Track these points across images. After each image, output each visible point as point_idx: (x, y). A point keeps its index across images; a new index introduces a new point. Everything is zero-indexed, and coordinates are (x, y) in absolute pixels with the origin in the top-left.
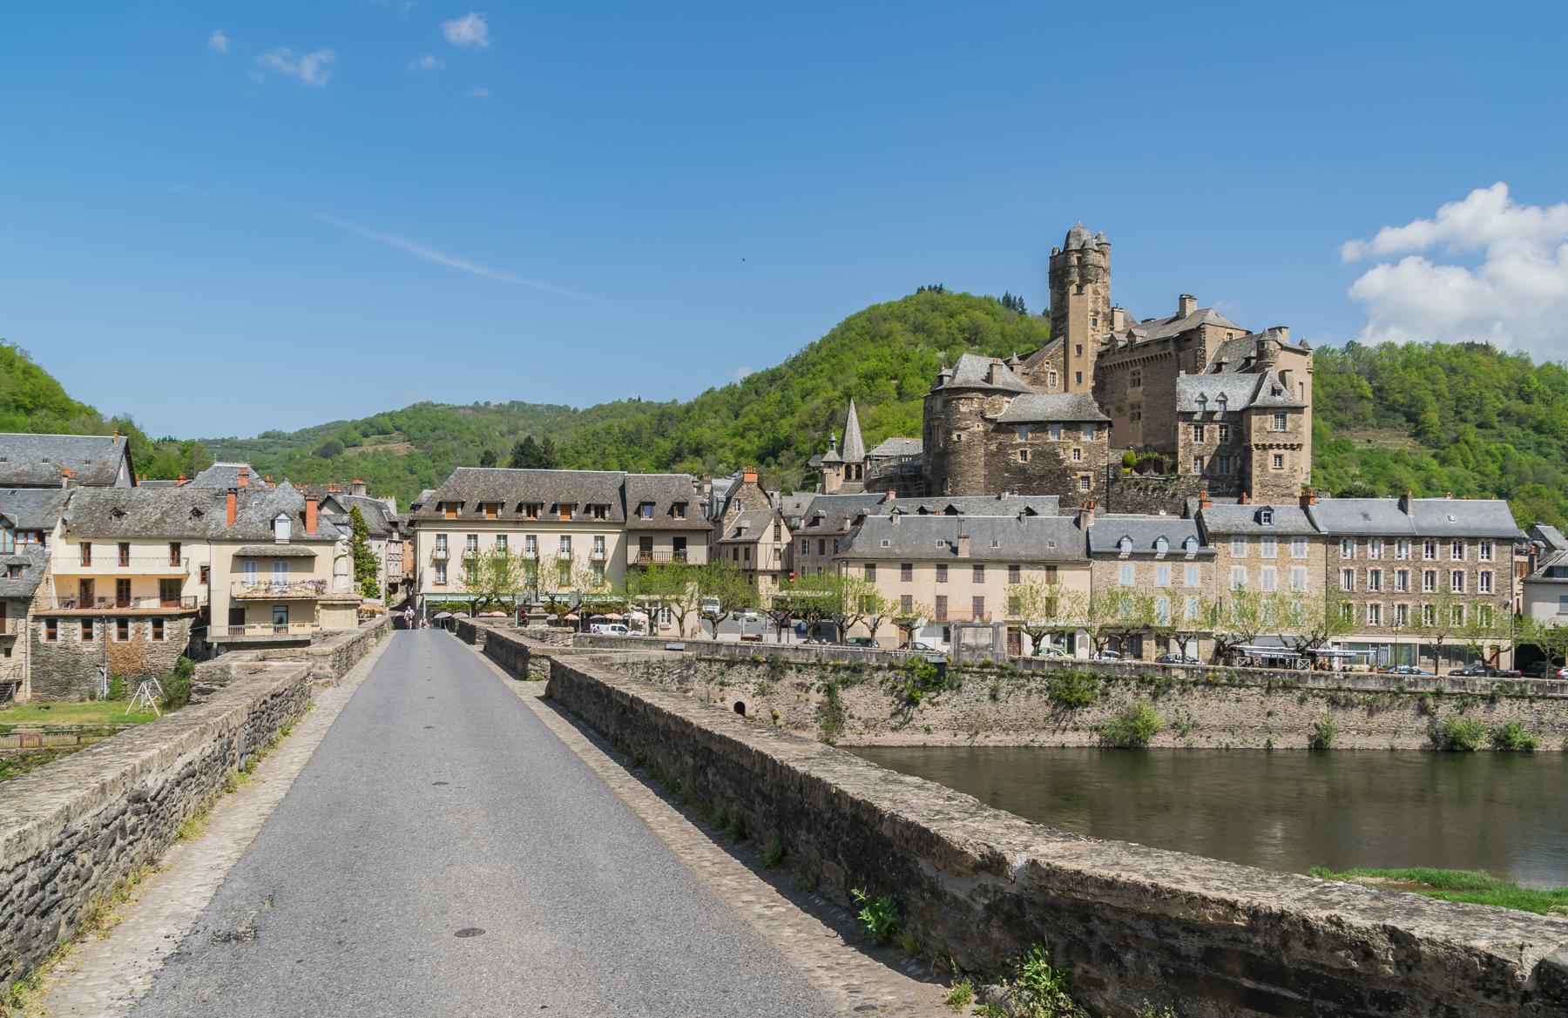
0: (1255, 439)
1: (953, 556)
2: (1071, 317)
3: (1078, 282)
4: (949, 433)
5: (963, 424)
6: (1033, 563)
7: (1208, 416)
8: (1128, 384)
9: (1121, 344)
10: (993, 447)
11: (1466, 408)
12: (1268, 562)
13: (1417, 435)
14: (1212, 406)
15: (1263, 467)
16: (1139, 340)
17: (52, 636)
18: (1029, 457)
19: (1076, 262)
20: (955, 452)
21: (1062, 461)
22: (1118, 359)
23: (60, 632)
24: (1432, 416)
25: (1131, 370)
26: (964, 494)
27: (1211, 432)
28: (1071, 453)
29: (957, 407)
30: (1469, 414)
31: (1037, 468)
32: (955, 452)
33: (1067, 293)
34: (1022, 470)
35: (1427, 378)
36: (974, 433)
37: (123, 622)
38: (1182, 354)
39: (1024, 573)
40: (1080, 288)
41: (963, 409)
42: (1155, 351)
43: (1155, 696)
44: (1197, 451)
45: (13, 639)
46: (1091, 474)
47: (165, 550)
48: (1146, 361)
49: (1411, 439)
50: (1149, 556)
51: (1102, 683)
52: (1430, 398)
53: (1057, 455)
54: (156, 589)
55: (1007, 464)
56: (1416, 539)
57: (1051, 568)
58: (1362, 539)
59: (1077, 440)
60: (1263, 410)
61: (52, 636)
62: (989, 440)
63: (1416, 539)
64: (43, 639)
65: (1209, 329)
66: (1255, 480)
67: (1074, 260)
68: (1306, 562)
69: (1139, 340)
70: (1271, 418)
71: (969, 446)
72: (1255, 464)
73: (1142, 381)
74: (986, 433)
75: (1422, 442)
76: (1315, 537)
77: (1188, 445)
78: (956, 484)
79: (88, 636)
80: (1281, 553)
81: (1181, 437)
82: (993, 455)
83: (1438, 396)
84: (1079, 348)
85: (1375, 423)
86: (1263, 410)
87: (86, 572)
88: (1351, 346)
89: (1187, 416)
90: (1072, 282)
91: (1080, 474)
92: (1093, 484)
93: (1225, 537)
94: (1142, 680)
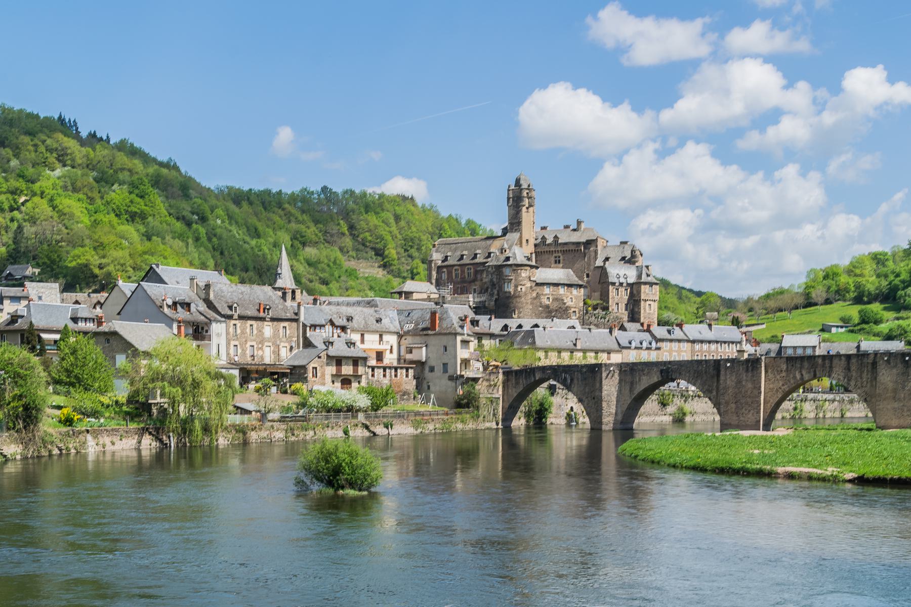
0: (642, 298)
1: (574, 347)
2: (524, 224)
3: (527, 206)
4: (516, 286)
5: (523, 283)
6: (603, 351)
7: (621, 284)
8: (553, 262)
9: (548, 242)
10: (534, 295)
11: (412, 247)
12: (675, 351)
13: (384, 266)
14: (622, 280)
15: (645, 309)
16: (560, 241)
17: (373, 375)
18: (551, 300)
19: (526, 195)
20: (519, 297)
21: (565, 304)
22: (547, 249)
23: (376, 374)
24: (392, 252)
25: (554, 255)
26: (523, 318)
27: (622, 292)
28: (569, 299)
29: (520, 273)
30: (413, 252)
31: (554, 306)
32: (519, 297)
33: (521, 210)
34: (547, 307)
35: (383, 222)
36: (527, 288)
37: (396, 369)
38: (587, 251)
39: (600, 355)
40: (527, 208)
41: (523, 275)
42: (572, 247)
43: (685, 401)
44: (616, 301)
45: (361, 376)
46: (577, 310)
47: (377, 337)
48: (564, 252)
49: (381, 269)
50: (641, 348)
51: (671, 397)
52: (389, 238)
53: (563, 300)
54: (374, 356)
55: (541, 303)
56: (717, 342)
57: (609, 353)
58: (702, 342)
59: (571, 293)
60: (645, 283)
61: (373, 375)
62: (533, 291)
63: (717, 342)
64: (370, 377)
65: (599, 239)
66: (642, 315)
67: (525, 193)
68: (685, 351)
69: (560, 241)
70: (648, 286)
71: (526, 294)
72: (642, 308)
73: (561, 261)
74: (531, 287)
75: (388, 272)
76: (688, 341)
77: (613, 298)
78: (520, 313)
79: (384, 376)
80: (679, 347)
81: (610, 294)
82: (535, 299)
83: (394, 237)
84: (527, 240)
85: (355, 255)
86: (645, 283)
87: (380, 347)
88: (324, 189)
89: (613, 284)
90: (524, 206)
91: (573, 310)
92: (578, 315)
93: (662, 340)
94: (682, 395)
